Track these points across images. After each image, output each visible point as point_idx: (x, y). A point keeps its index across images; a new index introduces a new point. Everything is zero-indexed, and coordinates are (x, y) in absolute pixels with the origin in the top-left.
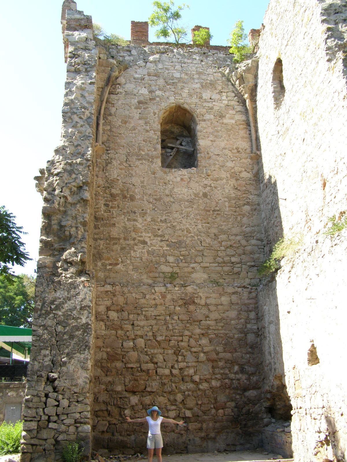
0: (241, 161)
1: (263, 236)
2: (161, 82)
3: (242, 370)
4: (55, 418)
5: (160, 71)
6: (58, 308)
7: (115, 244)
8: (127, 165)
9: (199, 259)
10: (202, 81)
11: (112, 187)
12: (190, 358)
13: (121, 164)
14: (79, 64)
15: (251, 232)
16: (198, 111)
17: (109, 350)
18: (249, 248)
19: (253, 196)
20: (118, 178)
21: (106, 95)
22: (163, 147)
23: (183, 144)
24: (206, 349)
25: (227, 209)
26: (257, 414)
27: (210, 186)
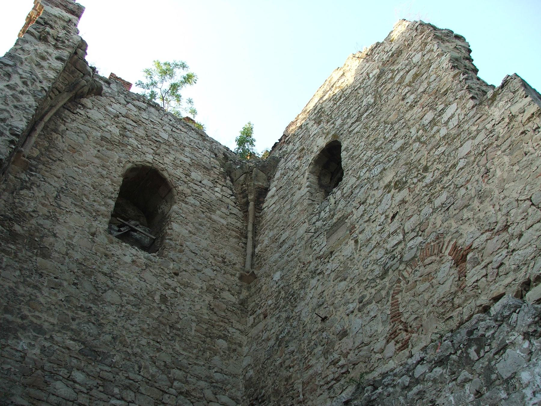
0: (225, 276)
13: (45, 197)
15: (223, 382)
16: (180, 188)
19: (234, 330)
25: (193, 333)
27: (174, 289)
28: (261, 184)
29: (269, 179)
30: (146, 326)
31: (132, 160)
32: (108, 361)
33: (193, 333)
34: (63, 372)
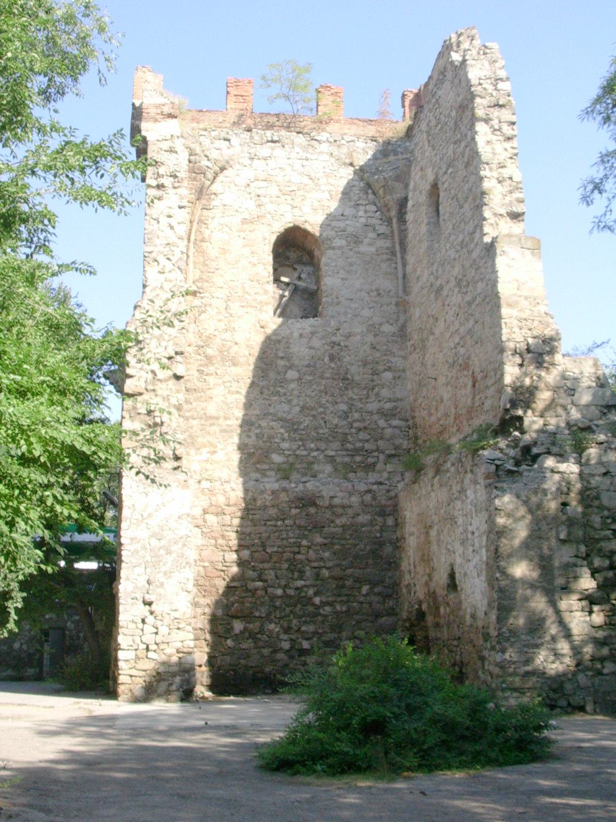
4: (155, 647)
7: (211, 425)
8: (227, 315)
10: (331, 188)
13: (219, 313)
15: (392, 409)
17: (206, 564)
20: (216, 333)
21: (198, 213)
23: (303, 276)
24: (330, 564)
28: (399, 195)
29: (406, 186)
31: (274, 230)
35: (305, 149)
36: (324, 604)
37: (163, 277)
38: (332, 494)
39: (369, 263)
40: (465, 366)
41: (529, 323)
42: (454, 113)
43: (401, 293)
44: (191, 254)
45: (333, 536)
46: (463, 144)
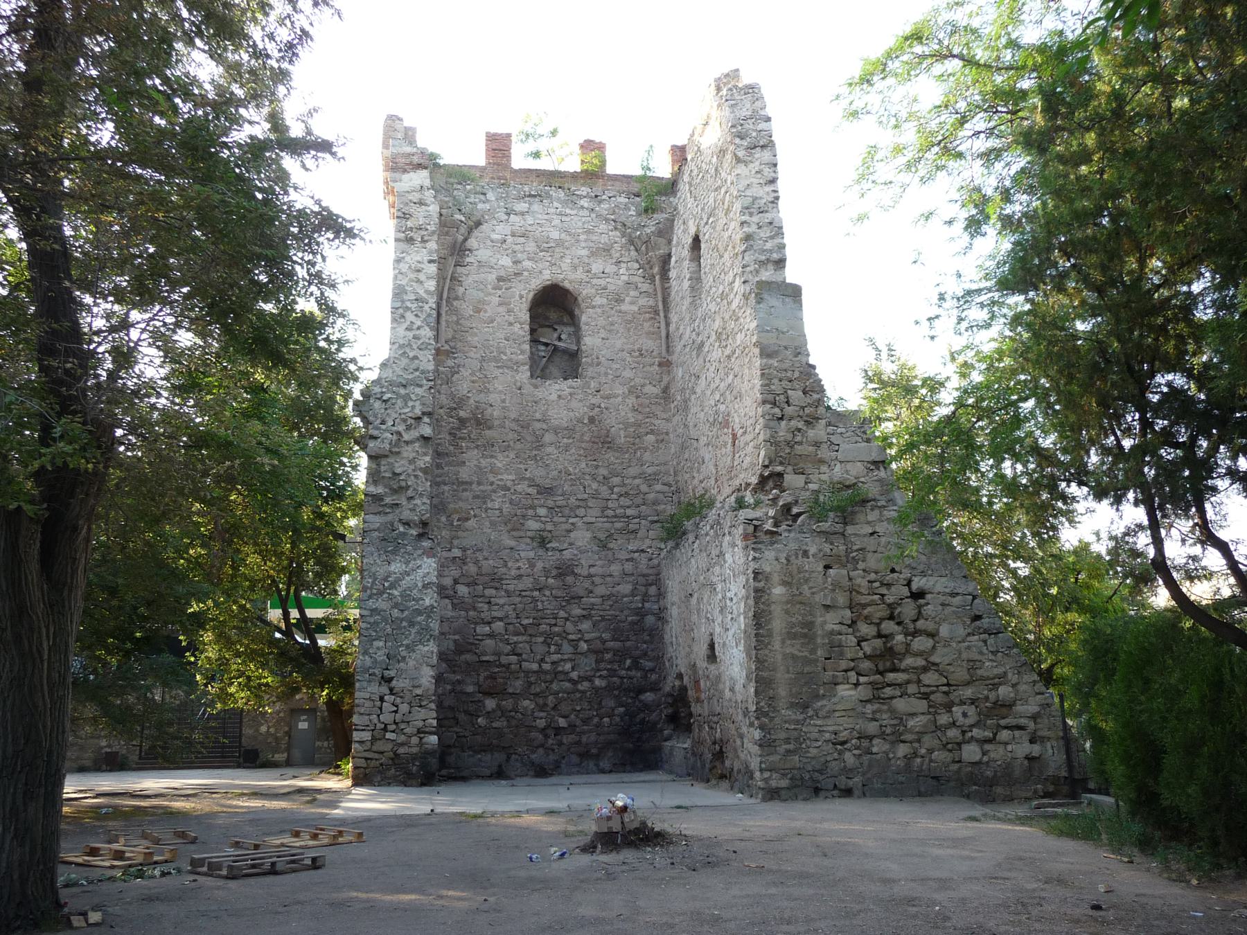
1: (671, 478)
2: (531, 246)
3: (636, 665)
4: (394, 727)
5: (529, 228)
6: (392, 586)
7: (465, 490)
9: (581, 512)
11: (461, 408)
12: (567, 648)
14: (411, 229)
15: (655, 474)
16: (584, 292)
17: (457, 637)
18: (651, 496)
22: (534, 341)
23: (563, 337)
24: (587, 636)
26: (655, 724)
29: (670, 241)
30: (582, 452)
32: (560, 492)
33: (623, 440)
34: (530, 512)
35: (565, 203)
36: (583, 679)
37: (410, 334)
38: (591, 562)
39: (631, 322)
40: (726, 424)
41: (789, 374)
42: (714, 160)
43: (664, 351)
44: (443, 313)
45: (592, 607)
46: (723, 191)
